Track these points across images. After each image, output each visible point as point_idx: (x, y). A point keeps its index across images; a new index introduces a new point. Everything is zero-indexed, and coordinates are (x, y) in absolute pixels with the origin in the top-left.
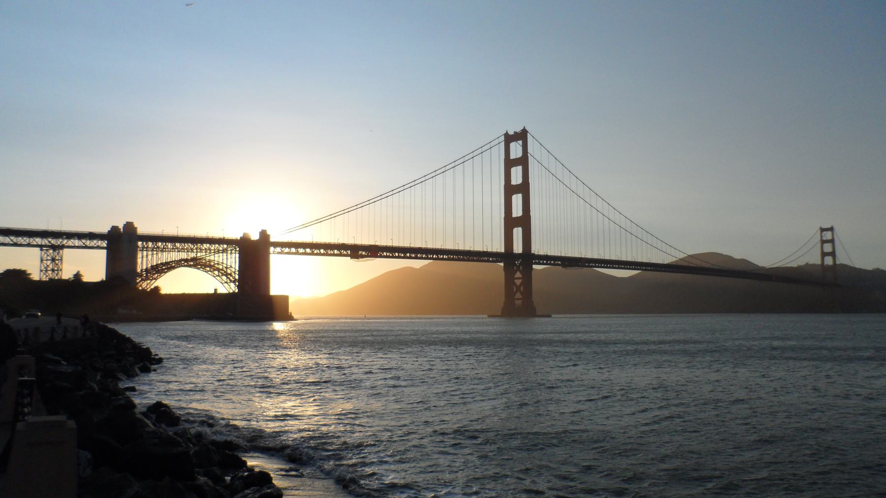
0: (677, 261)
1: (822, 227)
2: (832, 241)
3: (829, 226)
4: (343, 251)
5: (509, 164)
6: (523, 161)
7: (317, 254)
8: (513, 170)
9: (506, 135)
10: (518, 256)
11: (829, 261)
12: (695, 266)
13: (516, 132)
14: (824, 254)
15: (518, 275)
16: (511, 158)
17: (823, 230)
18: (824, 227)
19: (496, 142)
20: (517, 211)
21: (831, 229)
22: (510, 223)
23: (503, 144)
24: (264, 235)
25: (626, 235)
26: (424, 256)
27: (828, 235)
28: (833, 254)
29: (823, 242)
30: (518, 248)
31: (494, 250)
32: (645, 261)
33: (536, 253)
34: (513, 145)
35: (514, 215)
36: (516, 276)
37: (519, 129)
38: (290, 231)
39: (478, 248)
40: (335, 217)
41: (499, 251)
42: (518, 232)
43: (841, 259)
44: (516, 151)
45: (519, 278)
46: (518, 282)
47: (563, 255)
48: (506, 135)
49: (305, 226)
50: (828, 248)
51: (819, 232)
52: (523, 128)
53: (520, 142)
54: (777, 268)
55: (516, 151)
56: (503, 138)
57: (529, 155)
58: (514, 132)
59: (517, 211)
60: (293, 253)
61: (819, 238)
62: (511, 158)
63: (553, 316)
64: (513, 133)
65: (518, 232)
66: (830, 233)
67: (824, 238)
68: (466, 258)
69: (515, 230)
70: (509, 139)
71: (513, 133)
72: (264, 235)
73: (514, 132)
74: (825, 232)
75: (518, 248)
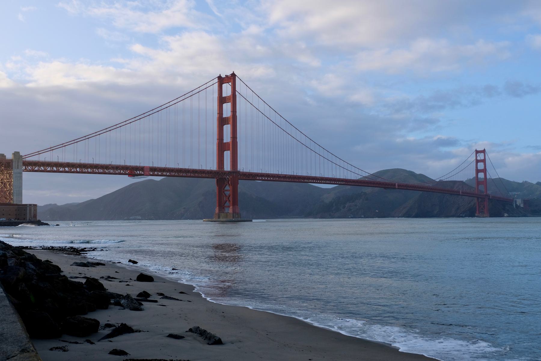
0: (362, 178)
1: (477, 150)
2: (484, 161)
3: (483, 149)
4: (95, 170)
5: (222, 100)
6: (233, 98)
7: (73, 172)
8: (225, 105)
9: (220, 78)
10: (229, 173)
11: (481, 175)
12: (371, 180)
13: (227, 75)
14: (478, 171)
15: (227, 188)
16: (223, 96)
17: (477, 152)
18: (478, 149)
19: (211, 83)
20: (227, 138)
21: (484, 151)
22: (222, 147)
23: (216, 86)
24: (16, 154)
25: (320, 157)
26: (168, 174)
27: (481, 157)
28: (484, 171)
29: (477, 161)
30: (227, 167)
31: (208, 168)
32: (353, 178)
33: (241, 171)
34: (224, 86)
35: (225, 141)
36: (226, 189)
37: (229, 73)
38: (39, 153)
39: (196, 167)
40: (77, 142)
41: (212, 169)
42: (227, 155)
43: (492, 174)
44: (227, 89)
45: (227, 190)
46: (227, 193)
47: (280, 173)
48: (220, 78)
49: (51, 149)
50: (481, 166)
51: (475, 153)
52: (232, 73)
53: (230, 83)
54: (454, 182)
55: (227, 89)
56: (216, 80)
57: (237, 93)
58: (226, 75)
59: (227, 138)
60: (42, 171)
61: (475, 158)
62: (223, 96)
63: (253, 221)
64: (225, 76)
65: (227, 155)
66: (483, 154)
67: (478, 158)
68: (200, 175)
69: (225, 152)
70: (221, 80)
71: (225, 76)
72: (16, 154)
73: (226, 75)
74: (479, 154)
75: (227, 167)
